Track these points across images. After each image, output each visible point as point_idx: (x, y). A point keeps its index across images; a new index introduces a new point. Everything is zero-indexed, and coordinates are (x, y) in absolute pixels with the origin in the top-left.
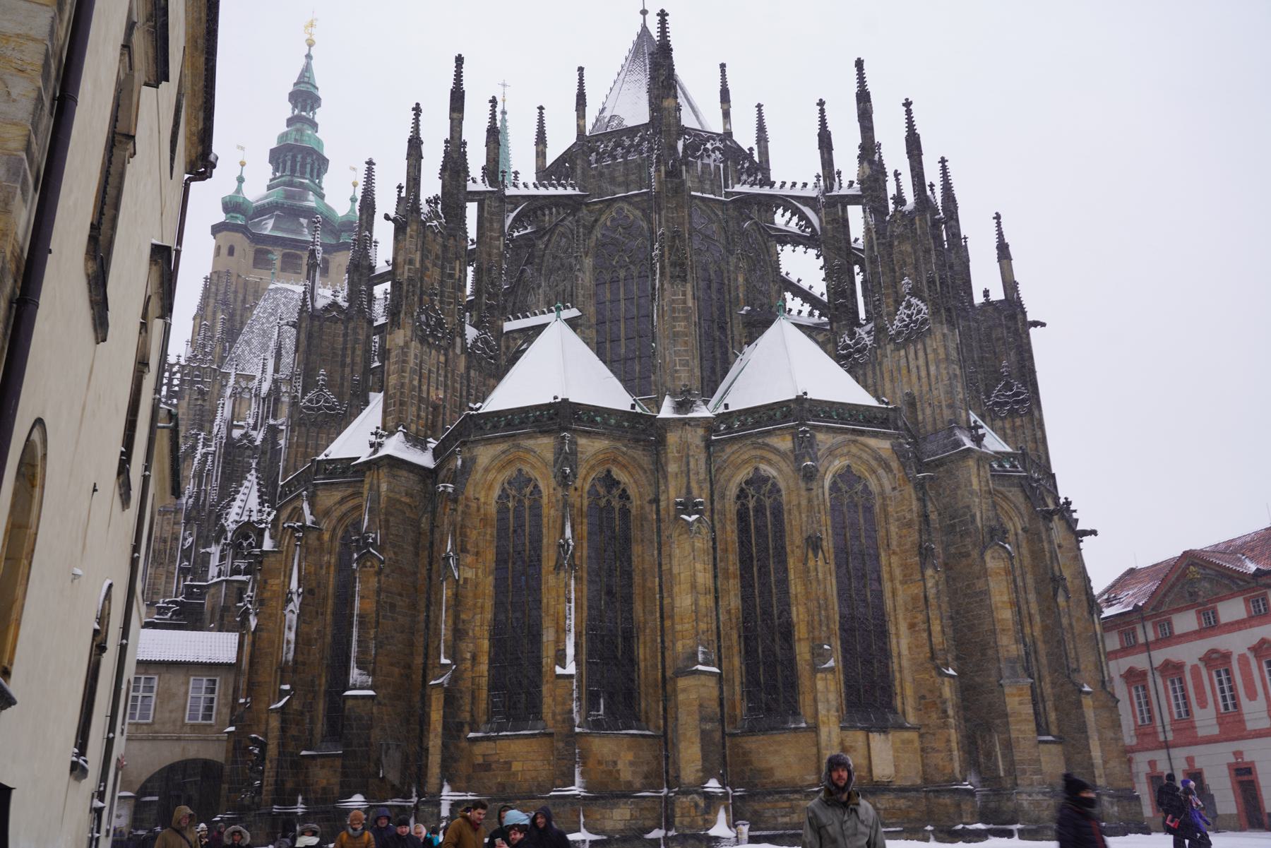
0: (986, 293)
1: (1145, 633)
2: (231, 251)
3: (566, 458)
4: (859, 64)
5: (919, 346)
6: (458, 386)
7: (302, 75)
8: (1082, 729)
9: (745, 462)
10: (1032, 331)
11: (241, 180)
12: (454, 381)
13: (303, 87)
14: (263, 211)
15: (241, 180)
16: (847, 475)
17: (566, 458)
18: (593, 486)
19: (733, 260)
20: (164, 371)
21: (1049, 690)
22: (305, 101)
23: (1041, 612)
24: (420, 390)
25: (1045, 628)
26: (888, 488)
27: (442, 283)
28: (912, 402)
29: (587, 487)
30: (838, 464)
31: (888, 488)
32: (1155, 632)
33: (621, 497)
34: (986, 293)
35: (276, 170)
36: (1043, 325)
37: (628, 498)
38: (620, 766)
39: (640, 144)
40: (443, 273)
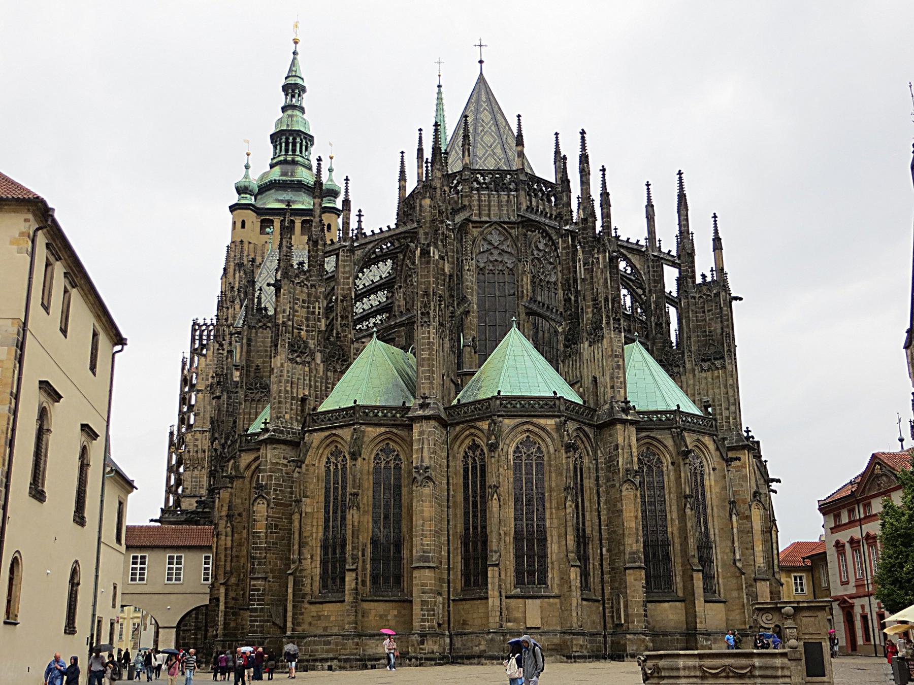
0: (704, 276)
1: (860, 513)
2: (243, 223)
3: (357, 442)
4: (583, 132)
6: (318, 384)
7: (290, 70)
10: (734, 302)
11: (247, 167)
12: (316, 381)
13: (291, 80)
14: (266, 187)
15: (247, 167)
16: (527, 443)
17: (357, 442)
18: (378, 454)
19: (520, 266)
20: (196, 330)
22: (293, 91)
23: (679, 518)
24: (292, 392)
25: (680, 529)
26: (552, 450)
27: (307, 319)
29: (373, 456)
31: (552, 450)
32: (865, 512)
33: (395, 459)
34: (704, 276)
35: (275, 147)
36: (741, 299)
37: (400, 460)
38: (389, 618)
40: (308, 313)
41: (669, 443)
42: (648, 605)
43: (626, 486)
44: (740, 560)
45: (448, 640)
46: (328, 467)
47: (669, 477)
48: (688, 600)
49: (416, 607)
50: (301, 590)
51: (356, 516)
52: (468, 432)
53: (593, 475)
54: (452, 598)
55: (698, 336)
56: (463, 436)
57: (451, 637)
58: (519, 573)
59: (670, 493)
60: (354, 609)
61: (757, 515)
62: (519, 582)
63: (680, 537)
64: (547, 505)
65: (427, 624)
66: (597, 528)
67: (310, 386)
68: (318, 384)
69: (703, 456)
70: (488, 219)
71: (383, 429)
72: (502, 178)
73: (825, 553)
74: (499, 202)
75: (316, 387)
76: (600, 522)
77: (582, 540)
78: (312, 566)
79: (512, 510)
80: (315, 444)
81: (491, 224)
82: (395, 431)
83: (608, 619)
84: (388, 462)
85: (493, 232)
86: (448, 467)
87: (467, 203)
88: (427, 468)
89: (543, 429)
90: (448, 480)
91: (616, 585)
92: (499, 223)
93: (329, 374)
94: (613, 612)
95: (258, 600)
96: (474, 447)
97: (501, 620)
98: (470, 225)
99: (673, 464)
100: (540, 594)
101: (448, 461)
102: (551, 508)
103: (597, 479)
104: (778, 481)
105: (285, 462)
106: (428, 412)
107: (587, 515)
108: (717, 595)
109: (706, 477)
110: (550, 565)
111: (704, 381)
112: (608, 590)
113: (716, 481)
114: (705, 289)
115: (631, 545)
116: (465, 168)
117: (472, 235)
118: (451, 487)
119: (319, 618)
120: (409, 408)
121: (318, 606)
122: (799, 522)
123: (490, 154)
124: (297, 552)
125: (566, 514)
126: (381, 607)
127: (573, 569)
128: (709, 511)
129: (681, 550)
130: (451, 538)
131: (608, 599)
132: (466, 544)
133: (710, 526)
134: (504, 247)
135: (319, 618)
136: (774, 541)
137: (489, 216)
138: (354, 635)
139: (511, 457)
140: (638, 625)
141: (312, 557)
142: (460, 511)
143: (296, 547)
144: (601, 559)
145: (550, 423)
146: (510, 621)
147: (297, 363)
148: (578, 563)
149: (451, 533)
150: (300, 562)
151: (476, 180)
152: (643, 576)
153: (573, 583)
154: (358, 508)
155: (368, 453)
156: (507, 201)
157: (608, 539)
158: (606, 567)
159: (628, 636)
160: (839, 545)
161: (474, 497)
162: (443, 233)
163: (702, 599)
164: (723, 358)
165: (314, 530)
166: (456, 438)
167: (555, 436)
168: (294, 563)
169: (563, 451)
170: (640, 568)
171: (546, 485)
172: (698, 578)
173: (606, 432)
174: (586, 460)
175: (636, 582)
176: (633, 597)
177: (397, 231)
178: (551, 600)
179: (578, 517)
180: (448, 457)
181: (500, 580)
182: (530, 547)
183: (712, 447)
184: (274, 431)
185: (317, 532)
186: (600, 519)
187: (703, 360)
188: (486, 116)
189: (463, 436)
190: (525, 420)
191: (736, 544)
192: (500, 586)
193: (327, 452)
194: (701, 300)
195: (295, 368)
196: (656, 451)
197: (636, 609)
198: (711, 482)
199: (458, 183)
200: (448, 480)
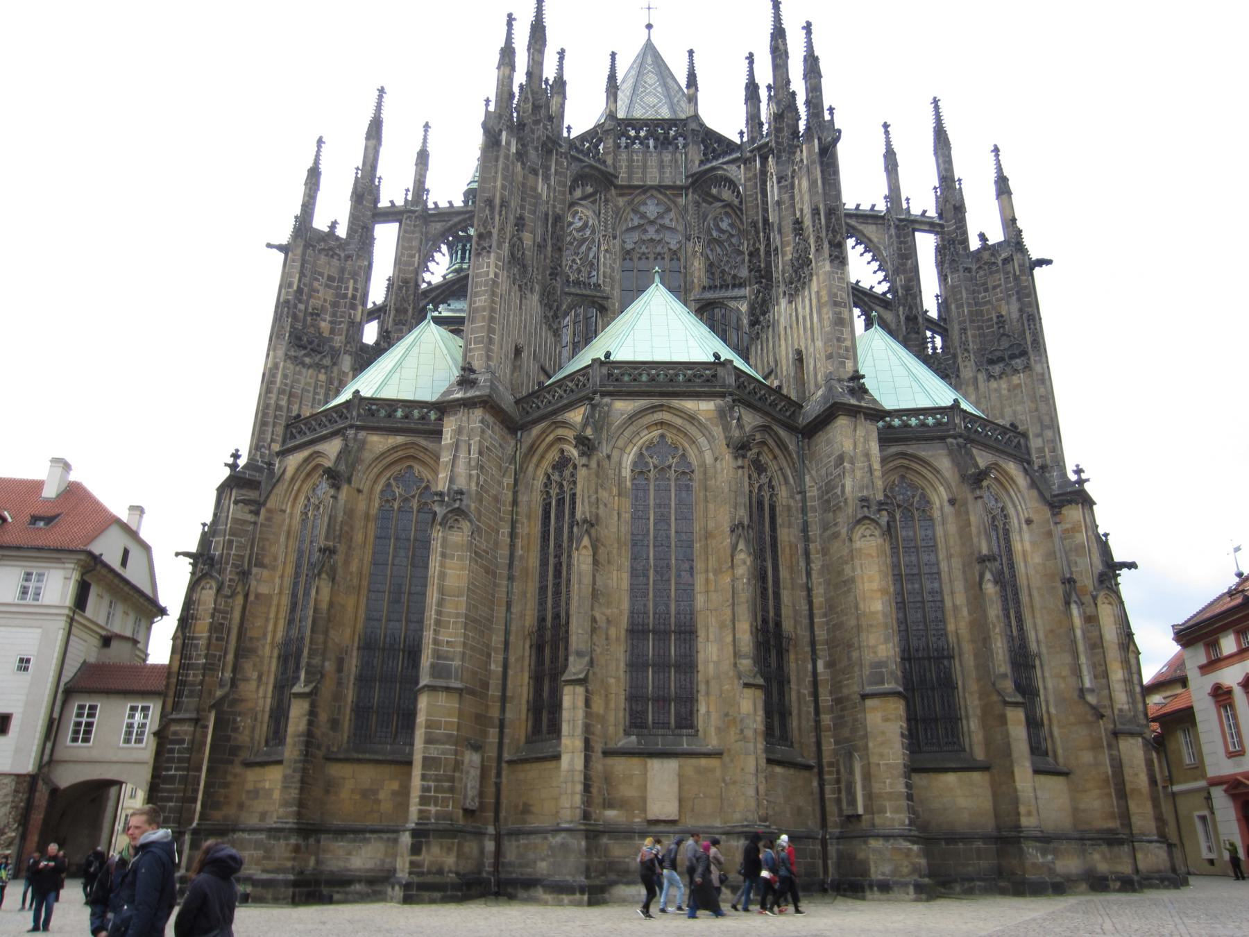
0: (982, 237)
5: (806, 293)
9: (551, 445)
18: (388, 485)
19: (691, 244)
21: (976, 702)
27: (335, 305)
28: (799, 358)
29: (378, 488)
30: (647, 437)
34: (982, 237)
36: (1049, 262)
38: (382, 795)
40: (338, 295)
41: (944, 464)
42: (916, 778)
43: (860, 530)
44: (1092, 691)
45: (490, 846)
46: (306, 514)
47: (946, 527)
48: (996, 766)
49: (417, 771)
50: (228, 739)
52: (551, 437)
53: (797, 520)
54: (506, 756)
55: (981, 328)
57: (498, 839)
59: (949, 557)
60: (298, 776)
61: (1106, 614)
62: (636, 723)
64: (699, 565)
65: (433, 809)
66: (805, 621)
71: (400, 439)
73: (1192, 707)
78: (258, 694)
79: (626, 577)
80: (290, 471)
81: (645, 189)
82: (423, 442)
83: (831, 808)
84: (406, 500)
85: (649, 202)
86: (515, 503)
88: (461, 492)
89: (691, 418)
90: (513, 527)
91: (846, 733)
92: (660, 188)
94: (839, 791)
95: (180, 760)
96: (563, 463)
99: (952, 502)
100: (678, 749)
101: (515, 493)
102: (707, 571)
103: (805, 528)
104: (1132, 566)
106: (471, 393)
107: (786, 597)
108: (1050, 760)
109: (1015, 537)
110: (702, 687)
111: (994, 396)
112: (829, 746)
113: (1033, 543)
114: (986, 255)
115: (874, 647)
116: (611, 116)
118: (519, 542)
119: (255, 794)
121: (258, 770)
122: (1157, 651)
124: (229, 667)
126: (365, 775)
128: (1024, 598)
129: (977, 667)
130: (512, 639)
131: (831, 764)
132: (539, 648)
133: (1028, 625)
135: (255, 794)
136: (1134, 669)
138: (291, 830)
139: (626, 473)
140: (894, 816)
141: (260, 677)
142: (532, 587)
143: (230, 657)
144: (815, 684)
145: (705, 408)
146: (609, 805)
147: (303, 364)
148: (761, 681)
149: (513, 628)
150: (234, 683)
157: (827, 642)
158: (825, 698)
159: (873, 843)
160: (1221, 695)
161: (558, 557)
162: (538, 138)
163: (1027, 764)
164: (1024, 353)
165: (270, 628)
166: (532, 449)
167: (717, 431)
168: (221, 685)
169: (728, 457)
171: (697, 527)
172: (1016, 721)
173: (821, 438)
174: (783, 493)
175: (885, 726)
176: (881, 755)
178: (704, 762)
179: (764, 591)
180: (516, 484)
181: (588, 715)
183: (1022, 481)
185: (275, 631)
186: (810, 603)
187: (991, 362)
188: (651, 79)
190: (655, 401)
191: (1083, 659)
192: (587, 728)
194: (982, 273)
195: (300, 373)
196: (918, 480)
197: (891, 782)
198: (1025, 544)
200: (513, 527)
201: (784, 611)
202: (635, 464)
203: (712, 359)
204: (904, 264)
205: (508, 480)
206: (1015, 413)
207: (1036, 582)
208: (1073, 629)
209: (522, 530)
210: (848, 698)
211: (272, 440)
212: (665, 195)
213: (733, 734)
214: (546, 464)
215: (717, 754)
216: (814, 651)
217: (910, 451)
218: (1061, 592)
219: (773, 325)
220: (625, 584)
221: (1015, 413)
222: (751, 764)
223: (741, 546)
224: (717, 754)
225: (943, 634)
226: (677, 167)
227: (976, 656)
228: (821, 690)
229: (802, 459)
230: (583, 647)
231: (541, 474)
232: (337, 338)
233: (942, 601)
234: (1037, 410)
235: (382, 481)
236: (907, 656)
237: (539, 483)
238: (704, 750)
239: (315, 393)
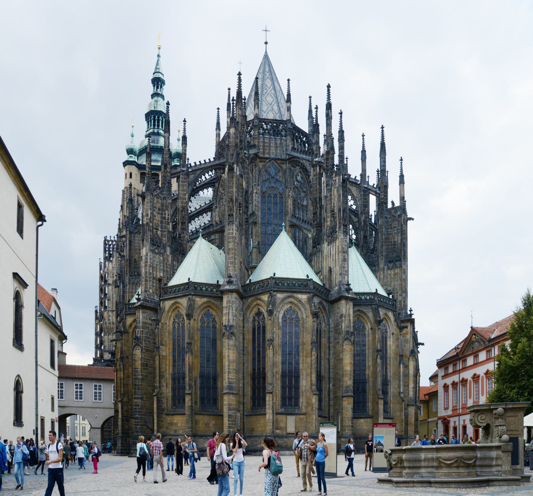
8: (377, 413)
23: (373, 365)
37: (216, 322)
39: (250, 131)
42: (354, 420)
51: (191, 358)
56: (252, 306)
58: (283, 398)
62: (283, 405)
63: (372, 378)
66: (327, 371)
67: (164, 271)
68: (168, 269)
69: (387, 325)
70: (267, 156)
72: (277, 126)
74: (276, 144)
75: (167, 271)
76: (329, 367)
77: (319, 378)
80: (167, 308)
81: (270, 159)
87: (256, 144)
92: (276, 159)
93: (175, 263)
97: (273, 428)
98: (258, 160)
105: (150, 322)
109: (388, 339)
111: (389, 277)
112: (332, 411)
113: (393, 342)
117: (259, 168)
120: (220, 285)
123: (270, 110)
125: (311, 361)
127: (314, 396)
134: (278, 177)
137: (269, 154)
142: (250, 358)
151: (262, 127)
152: (352, 402)
153: (314, 405)
154: (192, 353)
155: (197, 315)
156: (280, 144)
157: (333, 378)
163: (382, 416)
170: (351, 396)
172: (381, 402)
175: (348, 405)
177: (215, 163)
178: (301, 416)
182: (290, 382)
184: (143, 300)
186: (329, 365)
187: (390, 262)
189: (252, 306)
193: (173, 315)
198: (391, 343)
199: (251, 129)
201: (322, 368)
202: (283, 317)
203: (306, 278)
204: (364, 210)
205: (241, 318)
206: (395, 285)
207: (392, 356)
208: (400, 372)
209: (246, 337)
210: (338, 397)
211: (150, 288)
212: (278, 163)
213: (309, 409)
214: (253, 313)
215: (305, 414)
216: (329, 381)
217: (361, 309)
218: (398, 360)
219: (321, 251)
220: (280, 361)
221: (395, 285)
222: (314, 418)
223: (314, 350)
224: (305, 414)
225: (364, 375)
226: (283, 147)
227: (373, 382)
228: (331, 393)
229: (330, 312)
230: (271, 382)
231: (251, 316)
232: (164, 239)
233: (365, 364)
234: (401, 284)
235: (201, 316)
236: (354, 383)
237: (251, 319)
238: (301, 413)
239: (160, 266)
